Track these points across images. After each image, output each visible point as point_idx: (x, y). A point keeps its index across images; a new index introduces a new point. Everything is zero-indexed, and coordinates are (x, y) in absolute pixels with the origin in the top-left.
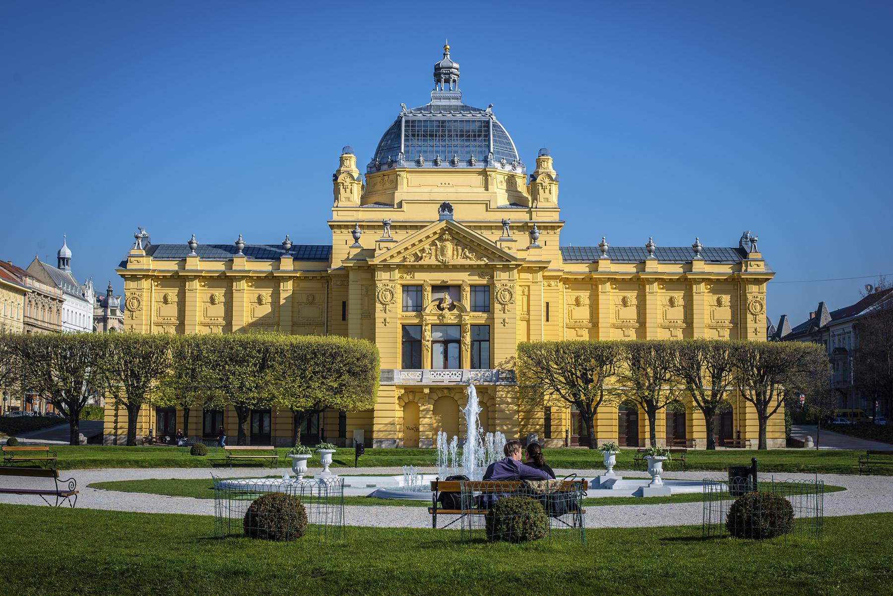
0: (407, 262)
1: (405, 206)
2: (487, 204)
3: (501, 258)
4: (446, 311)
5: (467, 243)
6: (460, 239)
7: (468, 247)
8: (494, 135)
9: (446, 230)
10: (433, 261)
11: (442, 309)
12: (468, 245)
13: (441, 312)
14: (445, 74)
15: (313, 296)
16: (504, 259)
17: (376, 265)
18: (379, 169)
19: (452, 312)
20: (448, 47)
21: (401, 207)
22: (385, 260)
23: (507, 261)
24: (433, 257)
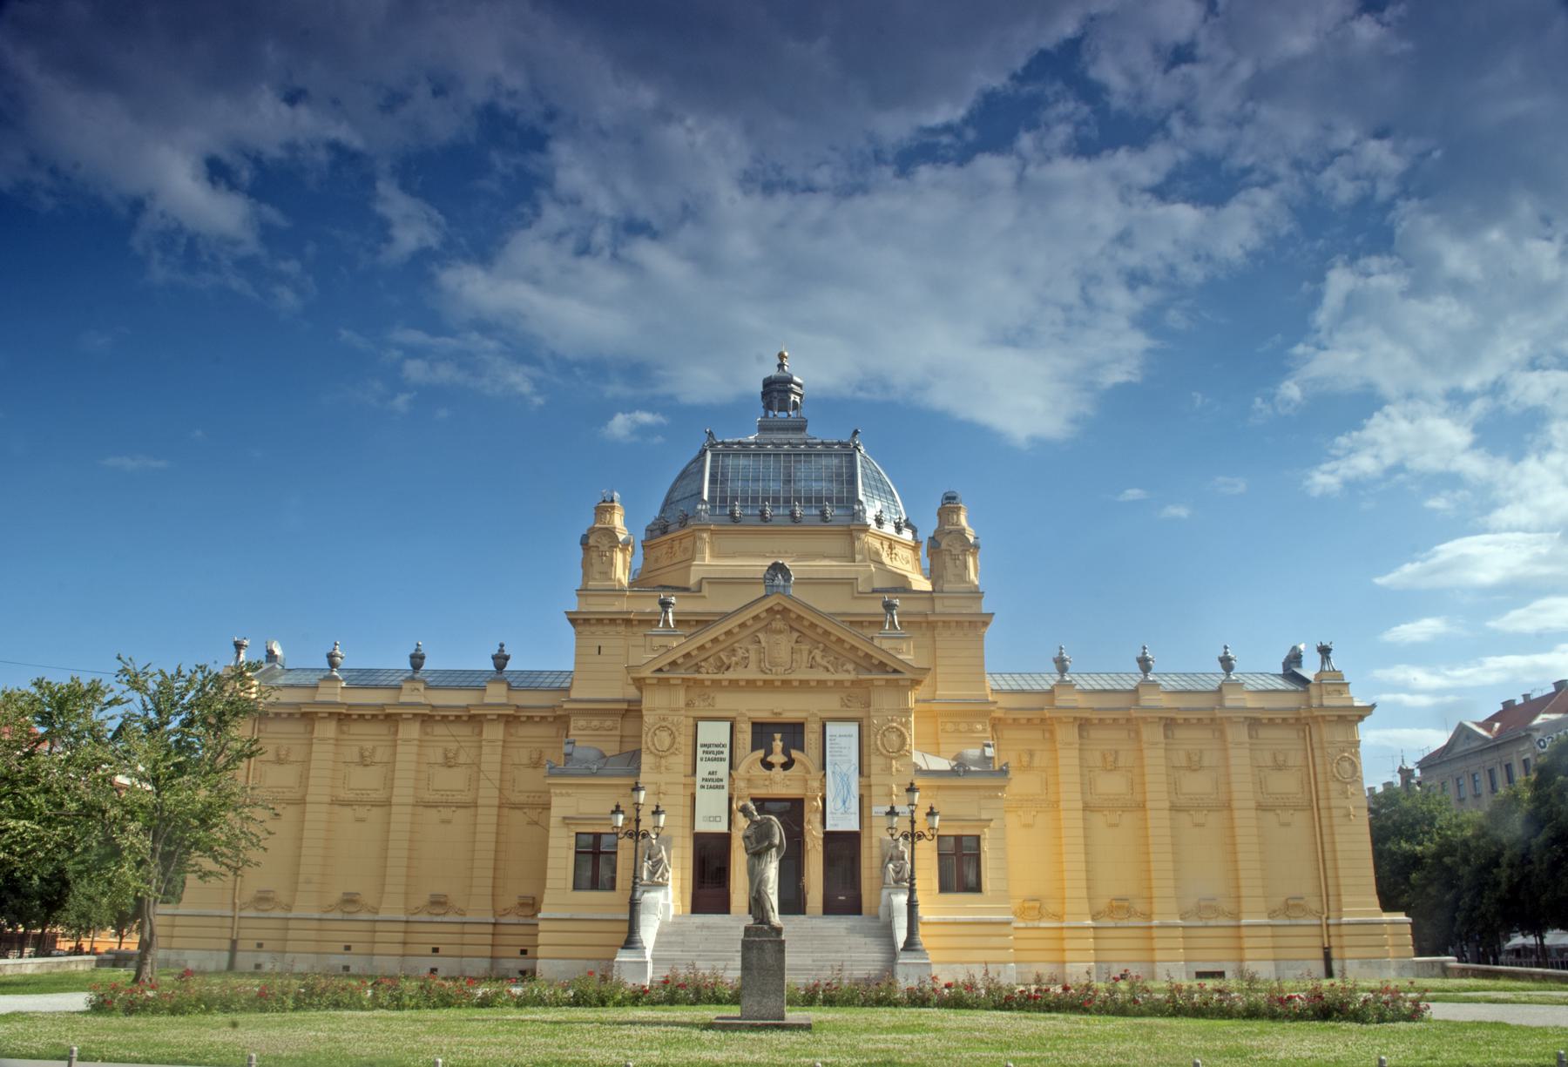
0: (700, 673)
1: (706, 589)
2: (852, 583)
3: (882, 667)
4: (777, 770)
5: (820, 639)
6: (805, 631)
7: (821, 645)
8: (865, 475)
9: (778, 612)
10: (752, 673)
11: (768, 766)
12: (819, 643)
13: (768, 772)
14: (779, 391)
15: (541, 752)
16: (888, 668)
17: (644, 679)
18: (664, 531)
19: (787, 772)
20: (786, 354)
21: (700, 591)
22: (660, 670)
23: (895, 671)
24: (753, 666)
